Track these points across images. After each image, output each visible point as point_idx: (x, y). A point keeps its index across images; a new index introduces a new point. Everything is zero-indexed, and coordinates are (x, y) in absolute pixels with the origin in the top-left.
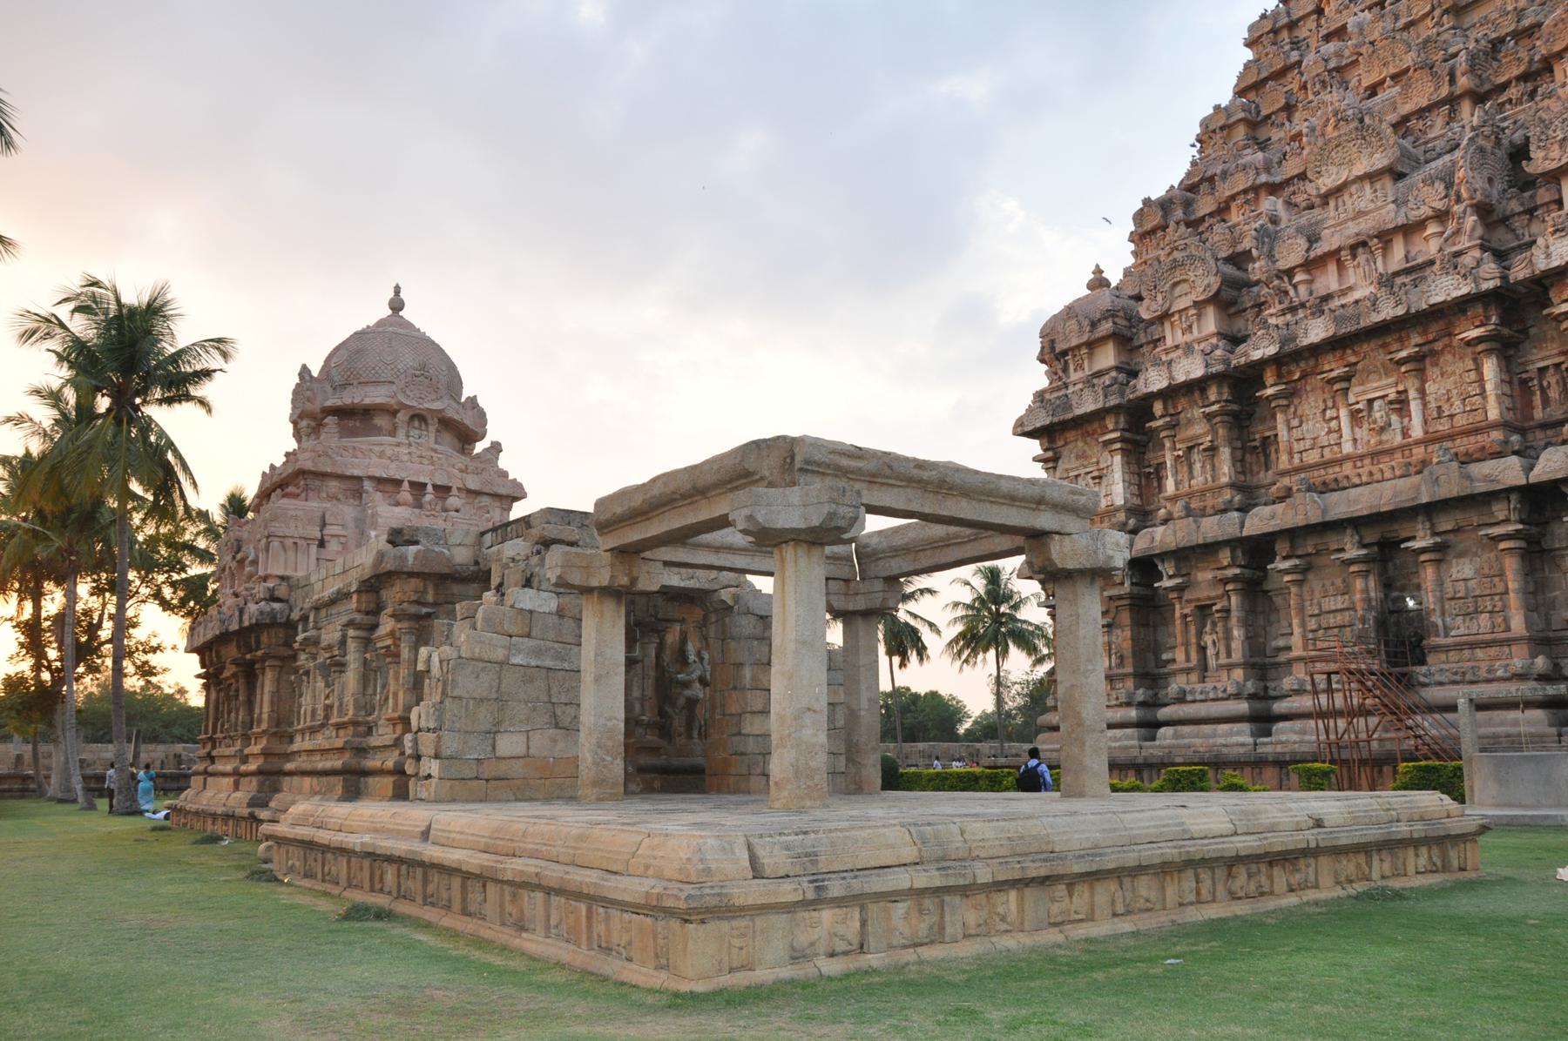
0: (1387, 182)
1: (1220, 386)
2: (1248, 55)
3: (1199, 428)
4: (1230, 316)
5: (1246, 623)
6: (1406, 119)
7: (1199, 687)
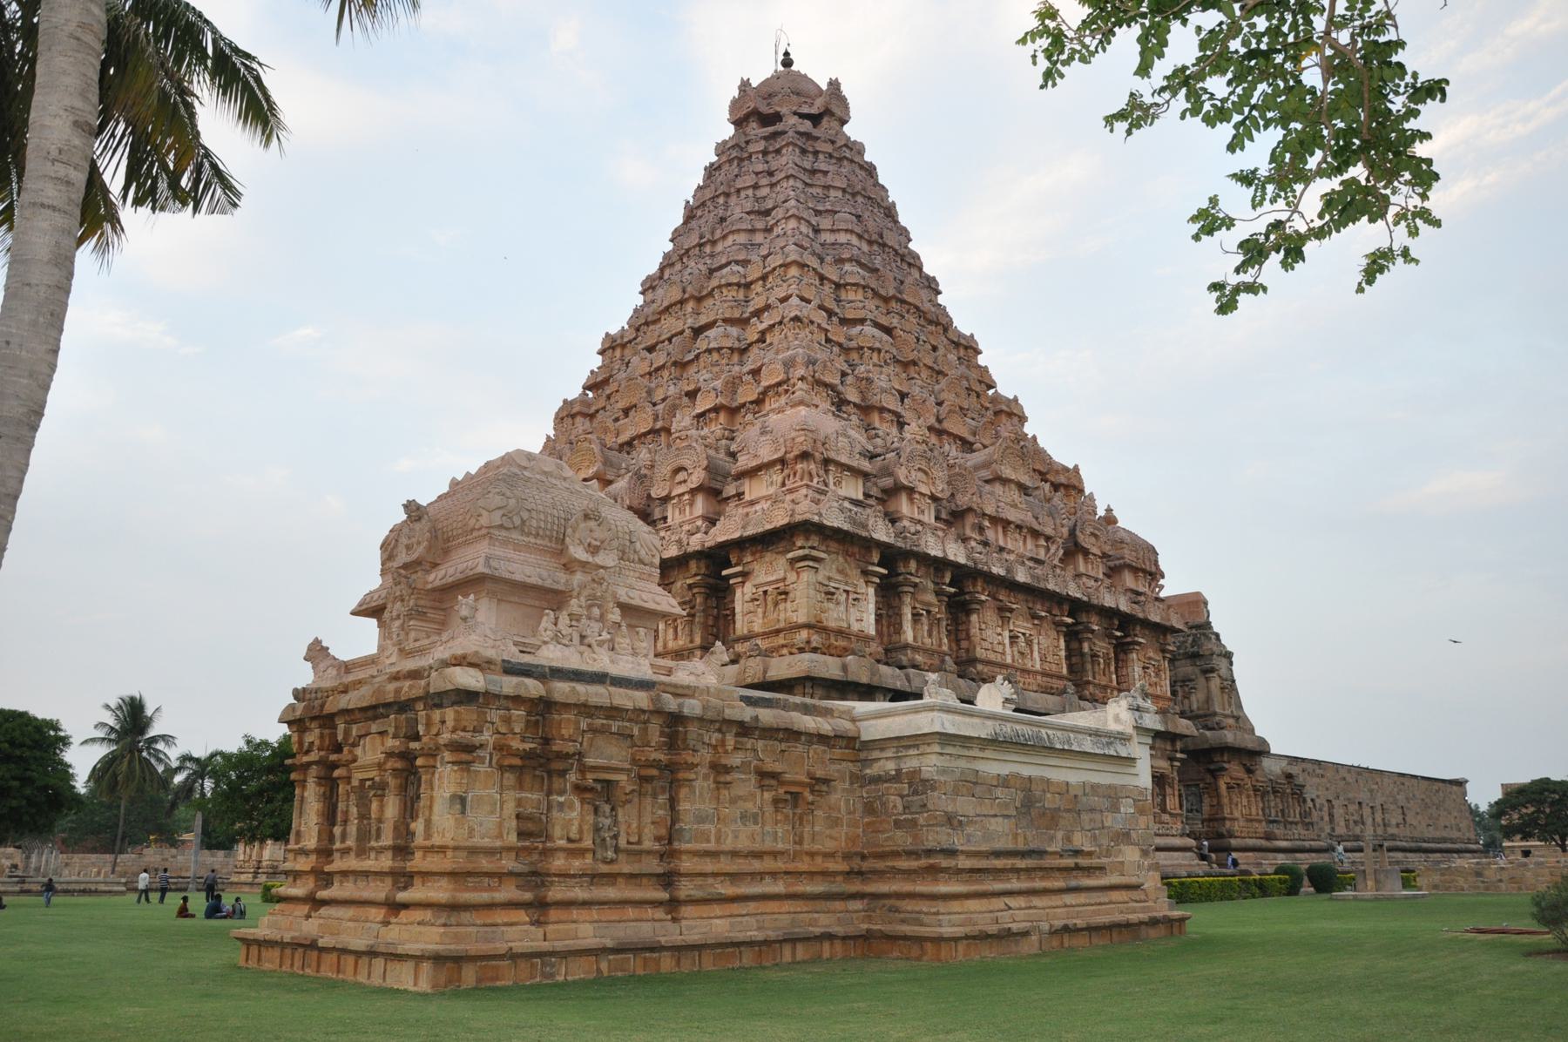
6: (633, 439)
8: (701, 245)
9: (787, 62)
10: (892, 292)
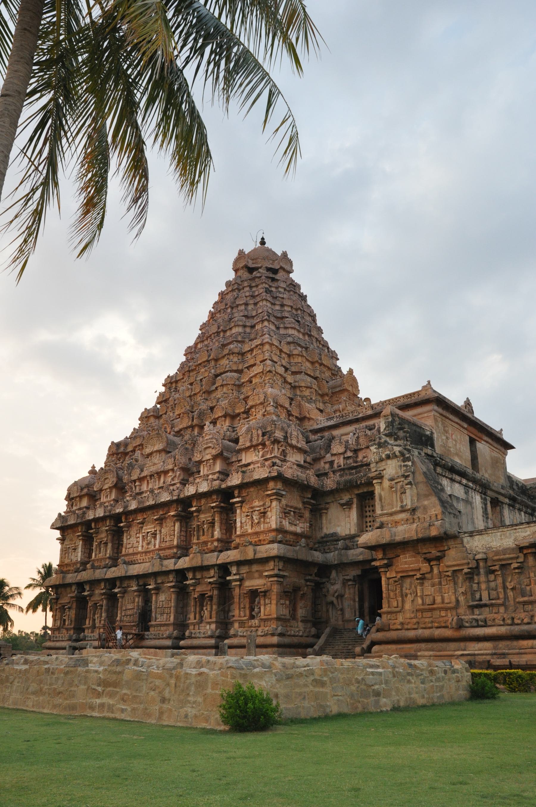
0: (163, 454)
1: (110, 520)
2: (163, 389)
3: (103, 535)
4: (123, 493)
5: (107, 611)
6: (181, 430)
7: (90, 635)
8: (218, 333)
9: (263, 242)
10: (317, 359)
